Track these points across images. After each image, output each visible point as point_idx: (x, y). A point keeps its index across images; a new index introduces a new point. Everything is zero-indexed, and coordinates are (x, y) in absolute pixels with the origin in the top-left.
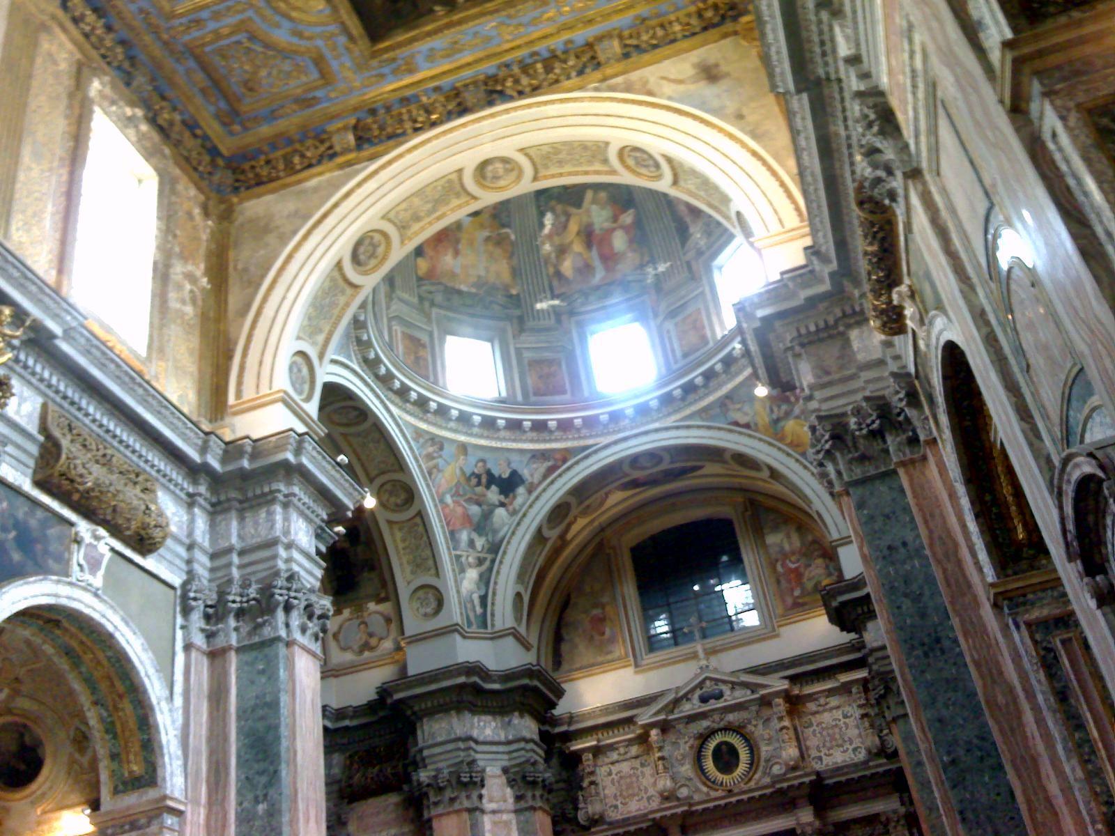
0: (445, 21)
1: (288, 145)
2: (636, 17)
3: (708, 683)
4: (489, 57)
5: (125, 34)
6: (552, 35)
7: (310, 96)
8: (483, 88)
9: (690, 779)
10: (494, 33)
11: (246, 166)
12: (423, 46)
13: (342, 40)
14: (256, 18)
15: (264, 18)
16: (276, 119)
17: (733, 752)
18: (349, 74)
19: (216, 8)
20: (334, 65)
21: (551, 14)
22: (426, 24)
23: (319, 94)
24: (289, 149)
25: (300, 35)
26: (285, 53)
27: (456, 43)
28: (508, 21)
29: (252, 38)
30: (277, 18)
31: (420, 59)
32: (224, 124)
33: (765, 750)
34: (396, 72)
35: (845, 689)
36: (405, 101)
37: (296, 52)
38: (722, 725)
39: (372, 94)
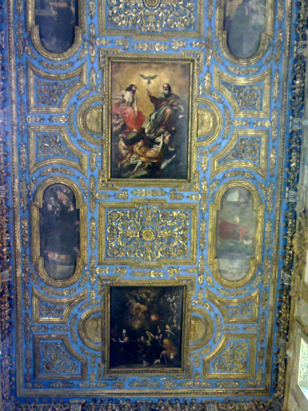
0: (146, 369)
1: (47, 403)
2: (227, 398)
4: (156, 393)
5: (13, 320)
6: (188, 393)
7: (71, 382)
8: (149, 407)
10: (163, 383)
11: (23, 405)
12: (131, 377)
13: (99, 360)
14: (69, 336)
15: (72, 336)
16: (50, 387)
18: (93, 378)
19: (55, 325)
20: (90, 370)
21: (190, 384)
22: (136, 367)
23: (75, 382)
24: (47, 405)
25: (82, 350)
26: (73, 356)
27: (145, 381)
28: (171, 380)
29: (63, 344)
30: (78, 339)
31: (126, 383)
32: (26, 381)
34: (114, 386)
36: (111, 400)
37: (76, 358)
39: (97, 392)
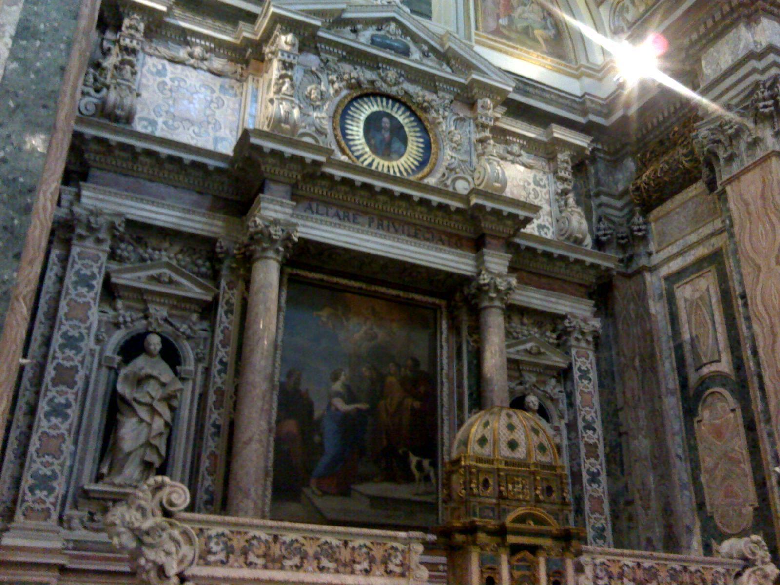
3: (393, 26)
9: (321, 132)
17: (398, 131)
33: (447, 155)
35: (547, 152)
38: (394, 90)
